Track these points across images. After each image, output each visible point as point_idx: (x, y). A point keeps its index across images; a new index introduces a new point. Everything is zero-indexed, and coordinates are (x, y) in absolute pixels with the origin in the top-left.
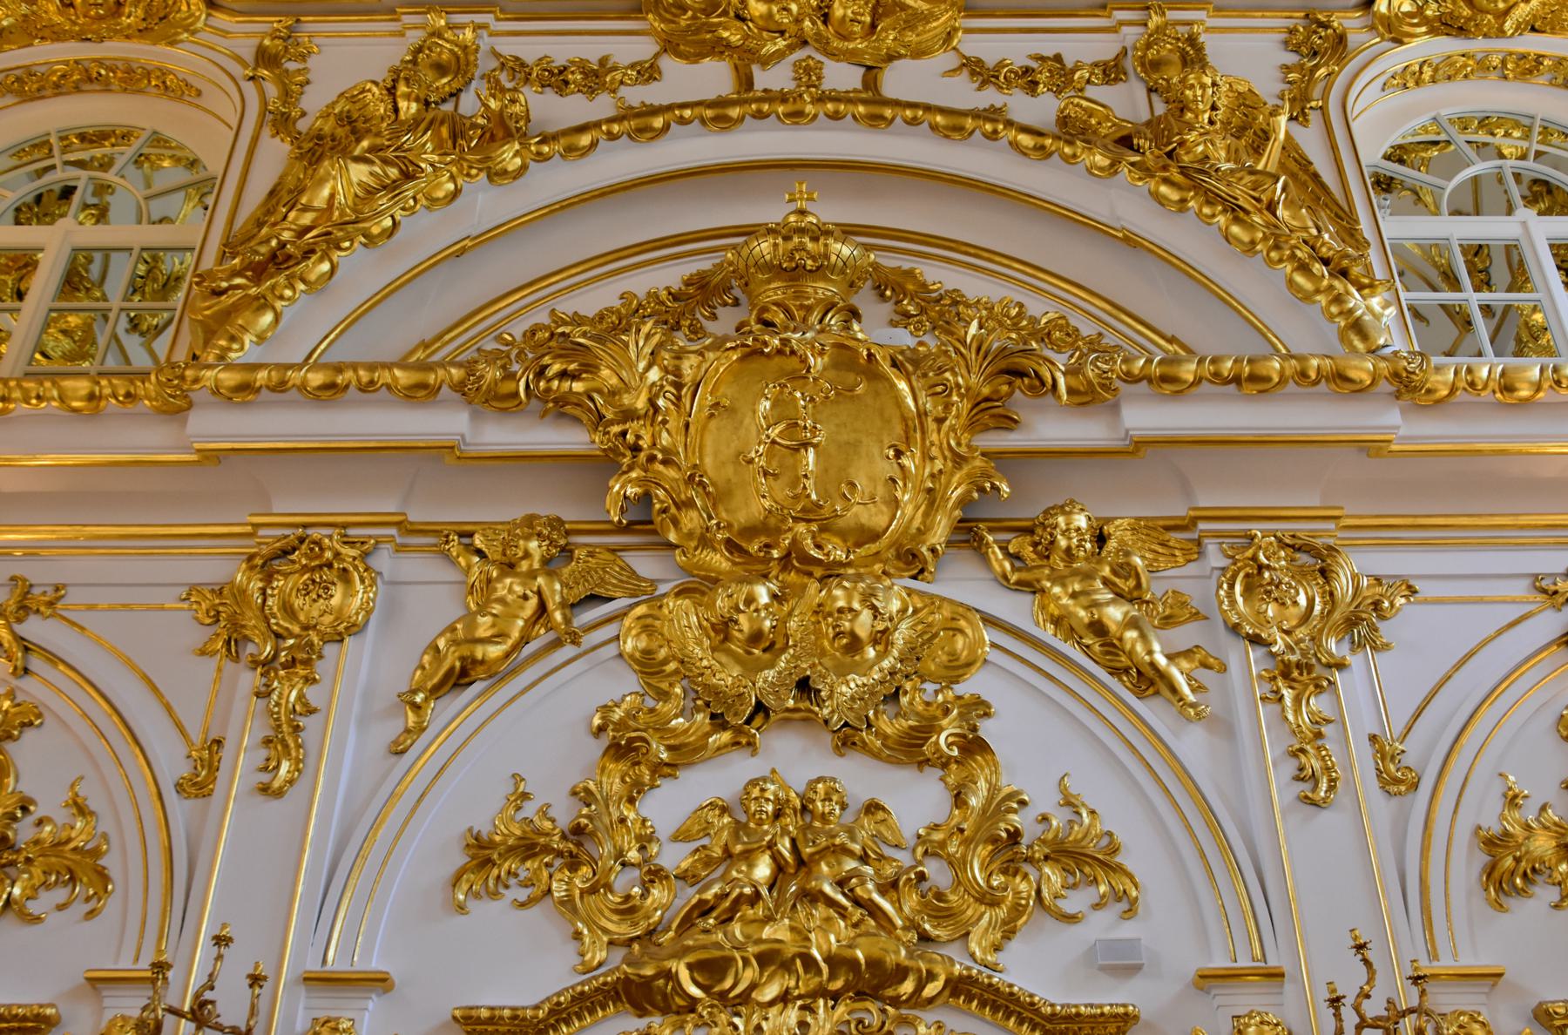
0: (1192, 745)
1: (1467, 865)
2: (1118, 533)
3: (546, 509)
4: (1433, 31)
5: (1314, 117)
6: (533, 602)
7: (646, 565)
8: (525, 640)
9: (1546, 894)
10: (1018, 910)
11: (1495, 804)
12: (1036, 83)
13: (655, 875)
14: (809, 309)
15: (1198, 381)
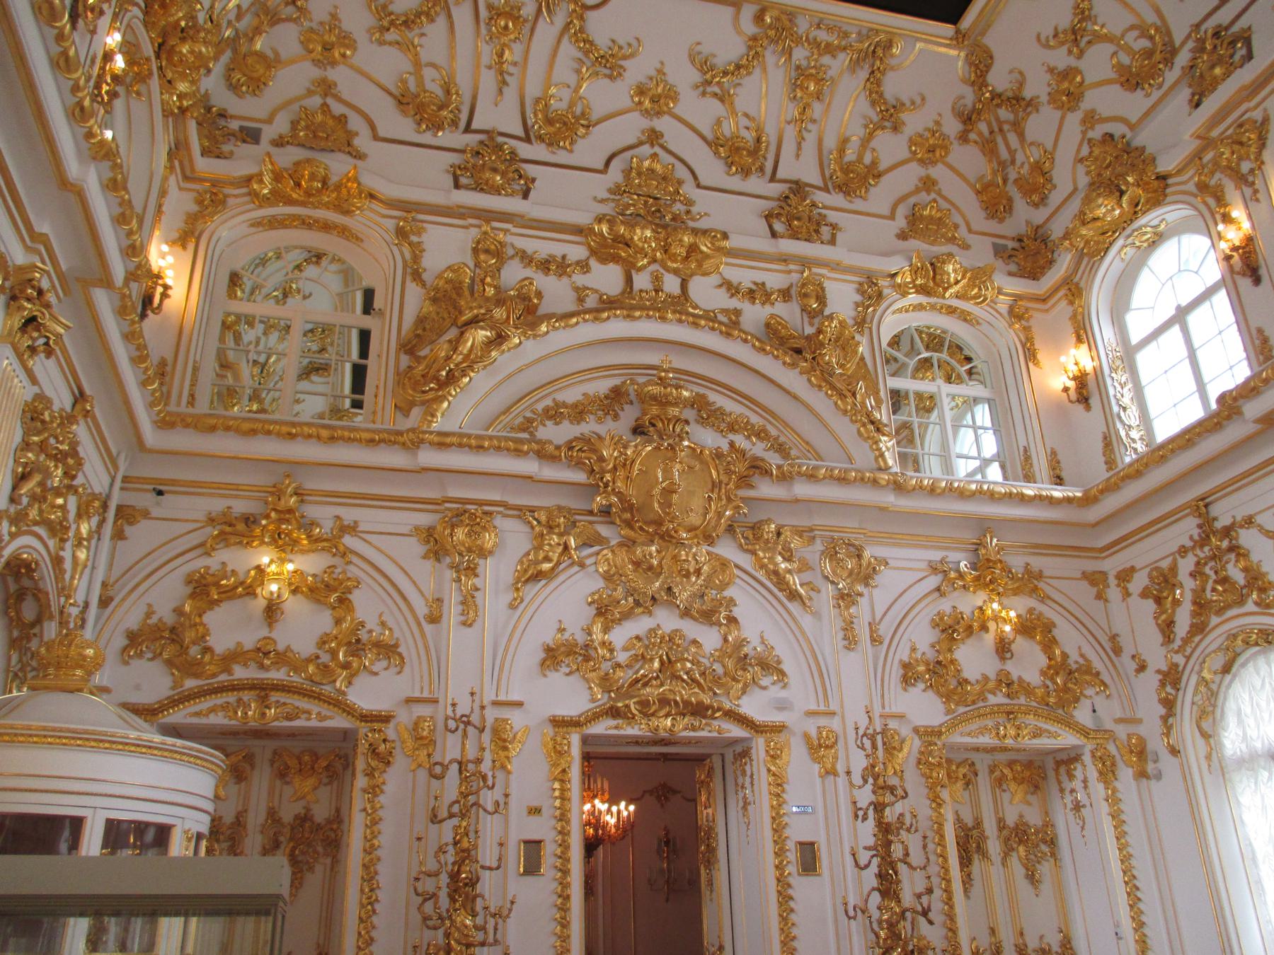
0: (806, 621)
1: (896, 673)
2: (787, 533)
3: (563, 502)
4: (917, 292)
5: (866, 331)
6: (561, 548)
7: (604, 530)
8: (558, 563)
9: (921, 686)
10: (746, 686)
11: (907, 651)
12: (754, 298)
13: (619, 665)
14: (669, 420)
15: (824, 478)
